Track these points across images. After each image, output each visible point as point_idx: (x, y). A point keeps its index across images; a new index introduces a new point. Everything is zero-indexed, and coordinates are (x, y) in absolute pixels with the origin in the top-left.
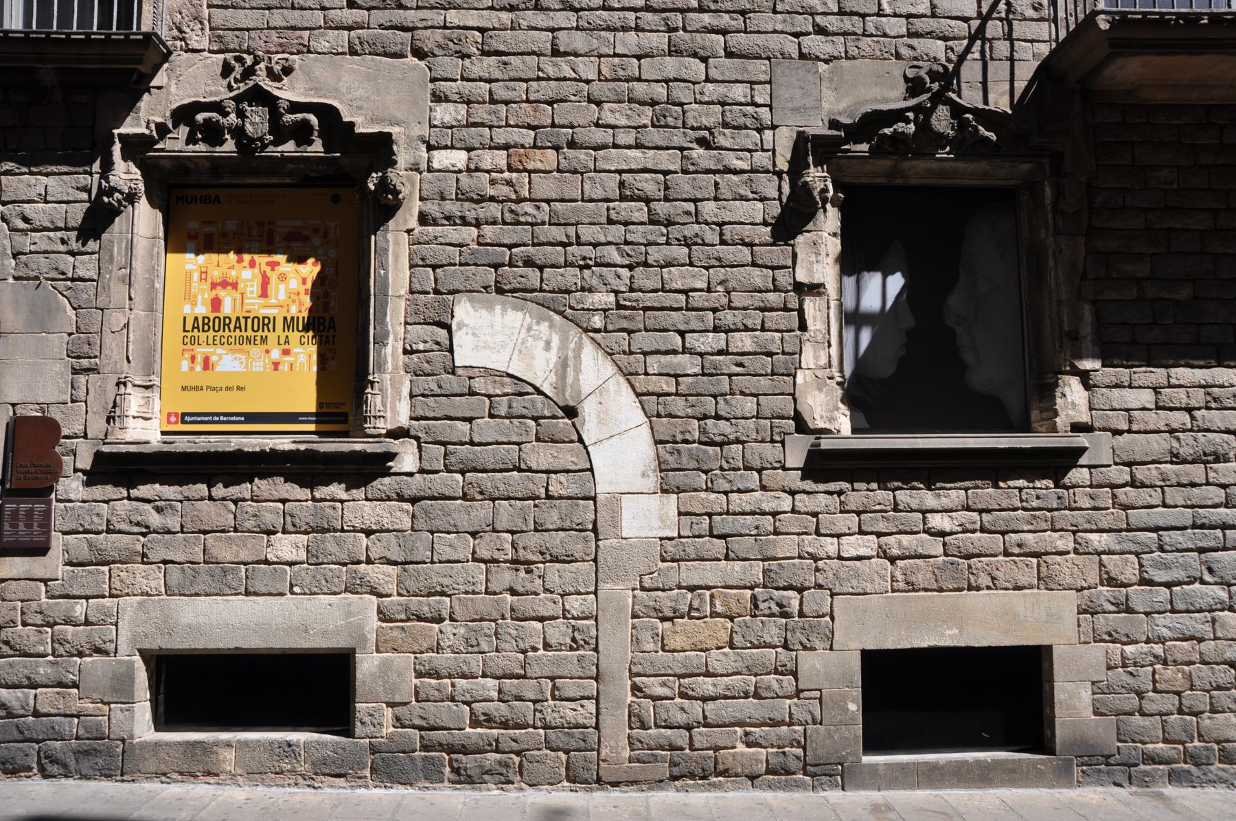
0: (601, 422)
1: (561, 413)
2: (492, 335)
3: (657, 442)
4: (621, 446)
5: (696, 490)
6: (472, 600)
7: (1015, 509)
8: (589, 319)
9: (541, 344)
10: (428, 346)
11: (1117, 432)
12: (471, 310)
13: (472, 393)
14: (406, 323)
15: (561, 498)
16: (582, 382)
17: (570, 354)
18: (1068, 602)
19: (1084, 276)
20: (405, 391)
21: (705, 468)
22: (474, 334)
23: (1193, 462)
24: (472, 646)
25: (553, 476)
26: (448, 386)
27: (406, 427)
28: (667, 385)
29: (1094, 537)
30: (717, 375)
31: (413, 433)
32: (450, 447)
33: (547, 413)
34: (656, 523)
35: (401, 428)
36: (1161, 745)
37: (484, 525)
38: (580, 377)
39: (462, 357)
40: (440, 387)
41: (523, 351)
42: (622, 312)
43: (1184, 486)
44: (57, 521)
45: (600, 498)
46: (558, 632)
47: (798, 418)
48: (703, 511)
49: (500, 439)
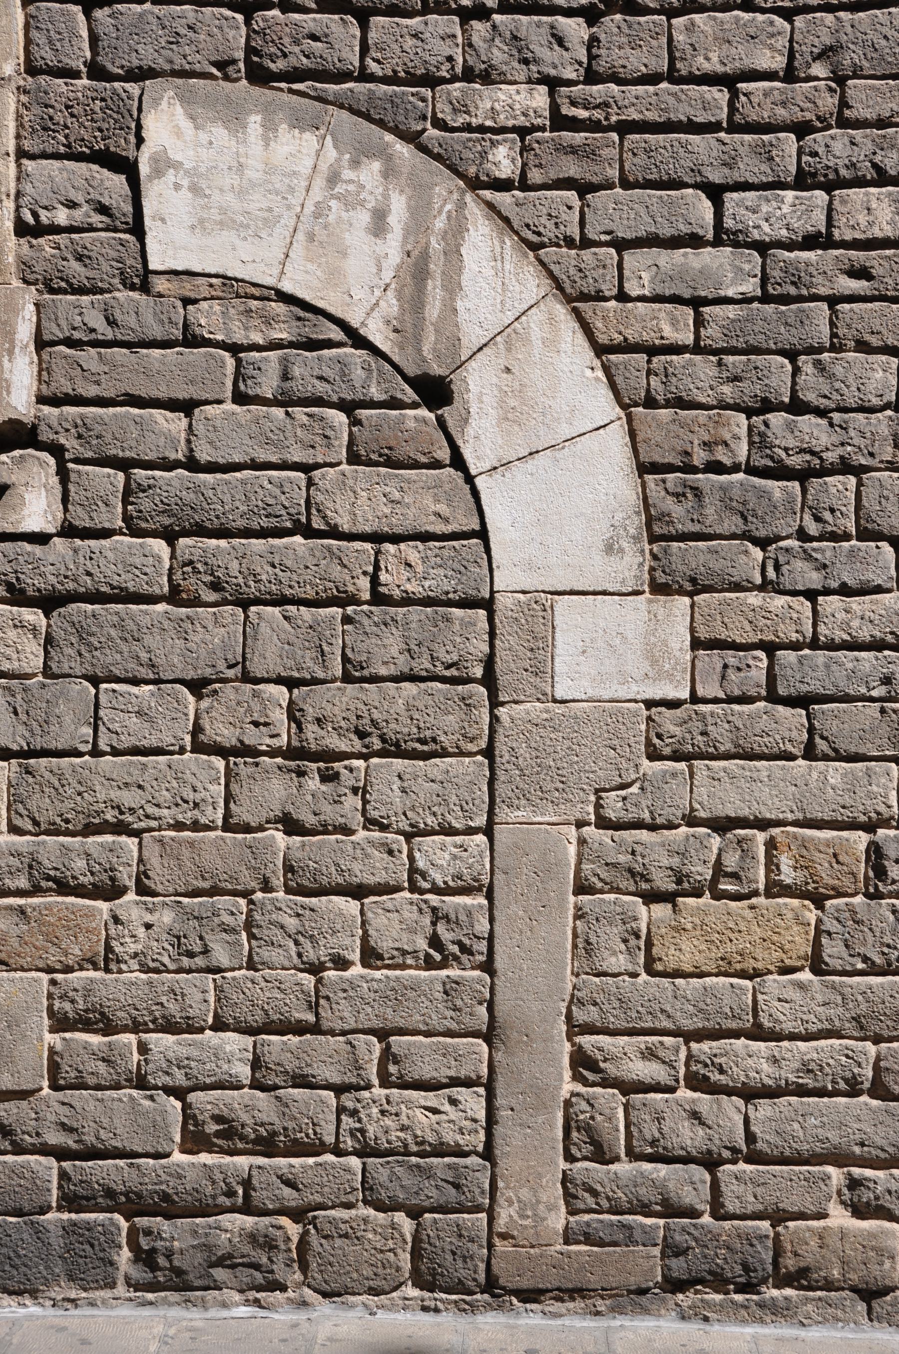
0: (508, 417)
1: (410, 395)
2: (241, 193)
3: (644, 469)
4: (555, 476)
5: (737, 587)
6: (191, 844)
8: (483, 155)
9: (364, 218)
10: (79, 216)
12: (186, 125)
13: (192, 340)
14: (21, 154)
15: (408, 601)
16: (463, 315)
17: (435, 245)
20: (25, 331)
21: (762, 533)
22: (194, 189)
24: (189, 954)
25: (390, 548)
26: (132, 321)
27: (28, 420)
28: (674, 325)
30: (800, 299)
31: (45, 435)
32: (139, 474)
33: (375, 393)
34: (636, 665)
35: (14, 424)
37: (221, 666)
38: (459, 305)
39: (169, 246)
40: (111, 322)
41: (318, 236)
42: (567, 136)
45: (503, 602)
46: (397, 923)
48: (754, 638)
49: (263, 456)
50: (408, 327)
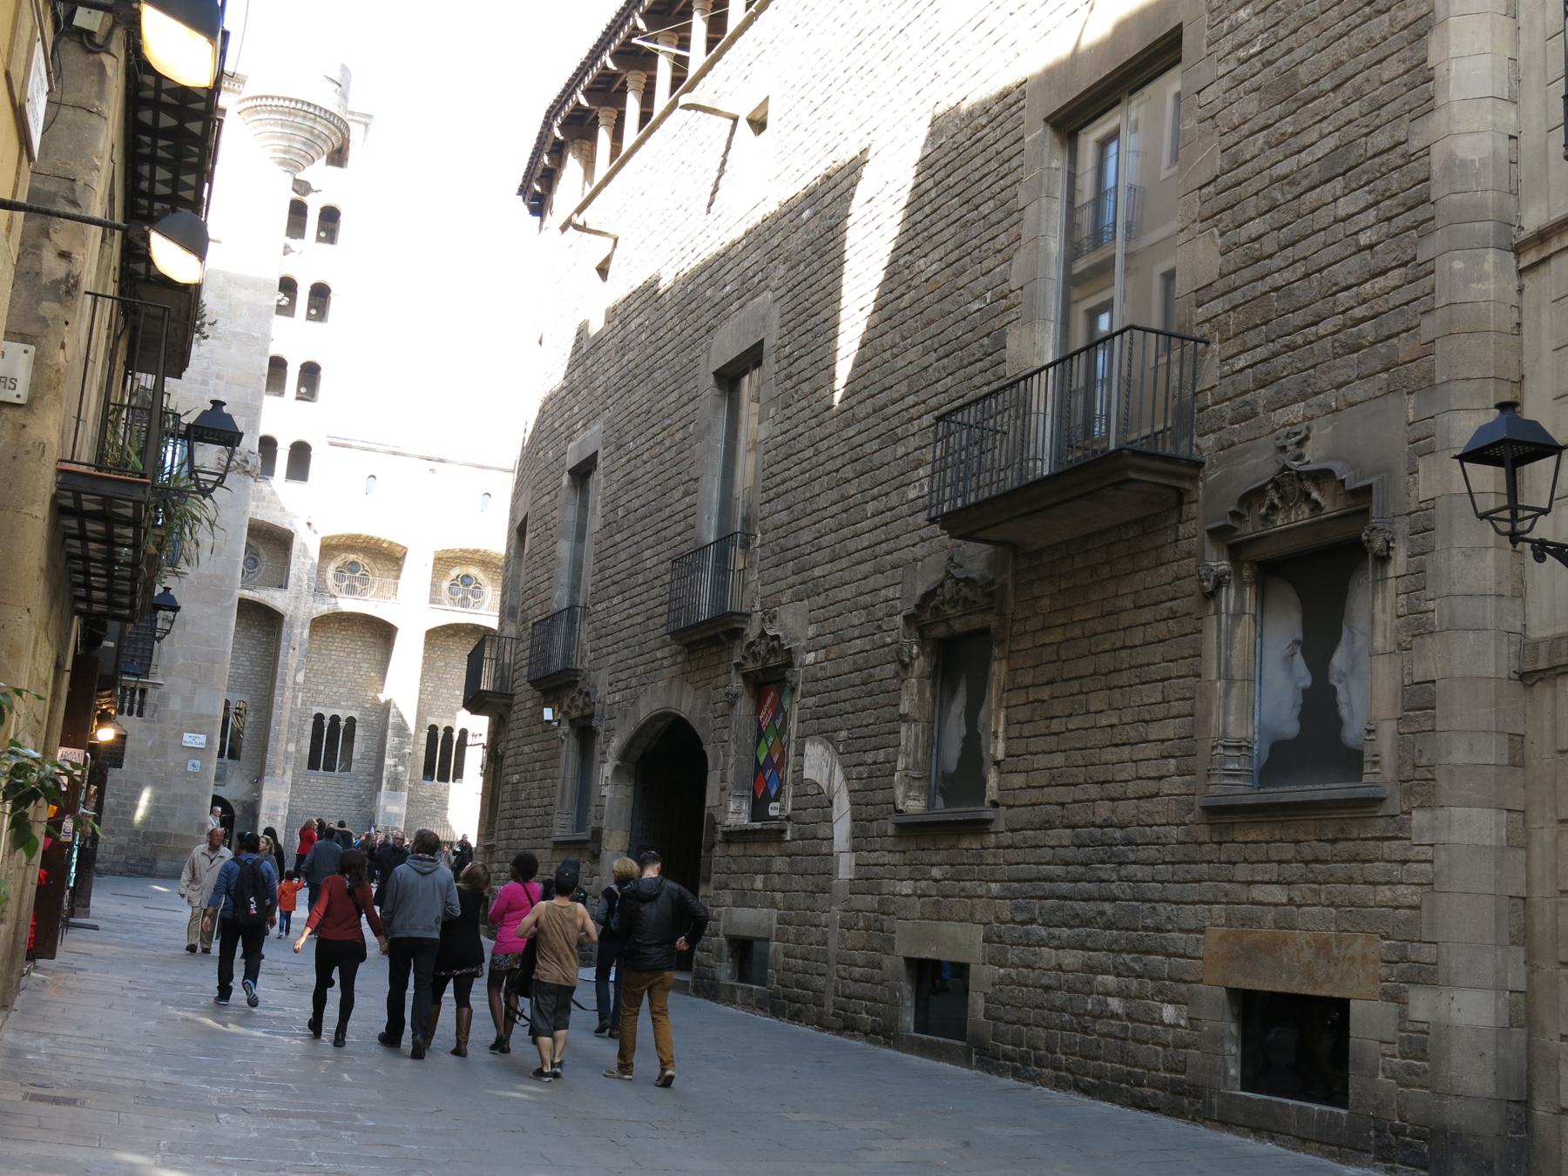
3: (854, 821)
11: (1010, 807)
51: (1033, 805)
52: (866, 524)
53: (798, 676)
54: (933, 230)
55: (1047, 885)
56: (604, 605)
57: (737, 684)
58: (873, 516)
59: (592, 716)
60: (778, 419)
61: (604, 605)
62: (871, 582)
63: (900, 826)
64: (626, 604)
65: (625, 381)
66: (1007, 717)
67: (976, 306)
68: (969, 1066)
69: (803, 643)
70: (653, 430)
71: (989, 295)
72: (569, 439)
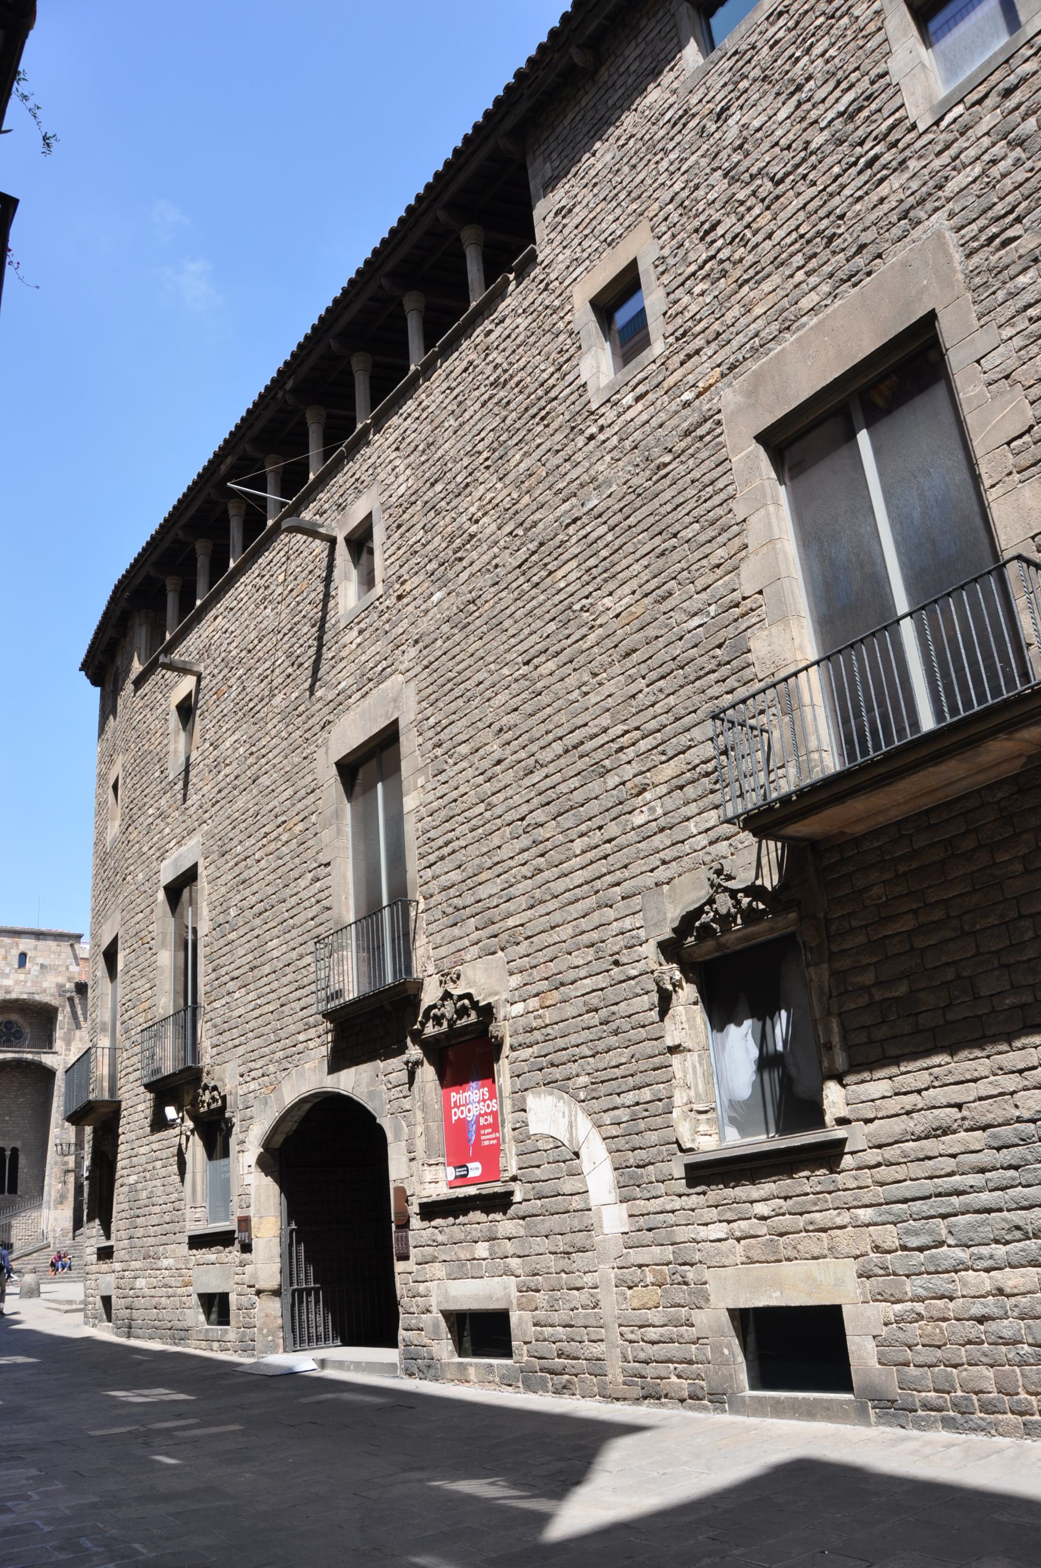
3: (616, 1169)
7: (807, 1194)
11: (867, 1121)
18: (851, 1267)
19: (831, 997)
23: (927, 1137)
29: (860, 1212)
36: (933, 1394)
39: (533, 1129)
43: (923, 1160)
44: (412, 1242)
47: (677, 1142)
50: (571, 1141)
51: (908, 1113)
52: (575, 862)
53: (502, 1028)
54: (618, 568)
55: (954, 1199)
56: (223, 1001)
57: (414, 1052)
58: (584, 852)
59: (223, 1108)
60: (429, 786)
61: (223, 1001)
62: (596, 918)
63: (690, 1168)
64: (251, 997)
65: (223, 794)
66: (843, 1026)
67: (696, 621)
68: (869, 1425)
69: (505, 995)
70: (265, 830)
71: (713, 607)
72: (161, 858)
